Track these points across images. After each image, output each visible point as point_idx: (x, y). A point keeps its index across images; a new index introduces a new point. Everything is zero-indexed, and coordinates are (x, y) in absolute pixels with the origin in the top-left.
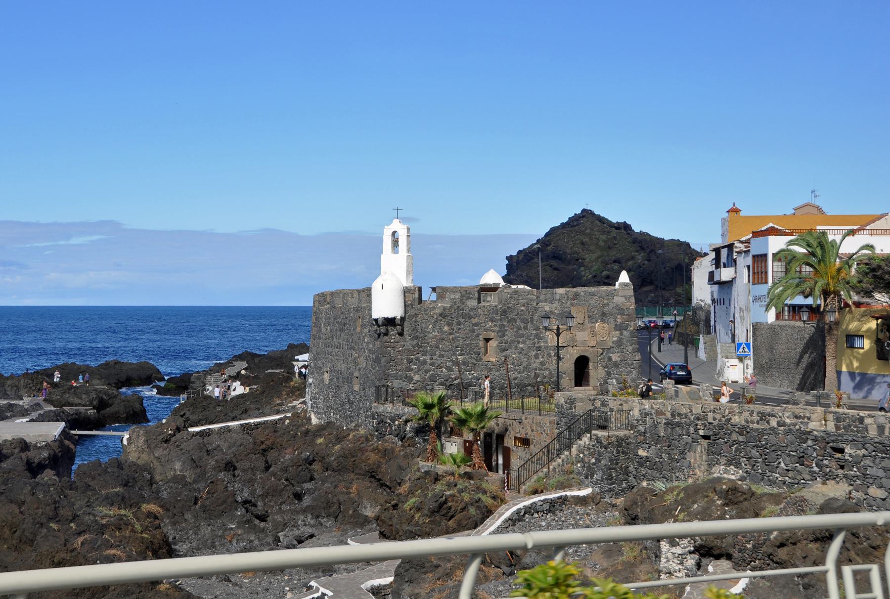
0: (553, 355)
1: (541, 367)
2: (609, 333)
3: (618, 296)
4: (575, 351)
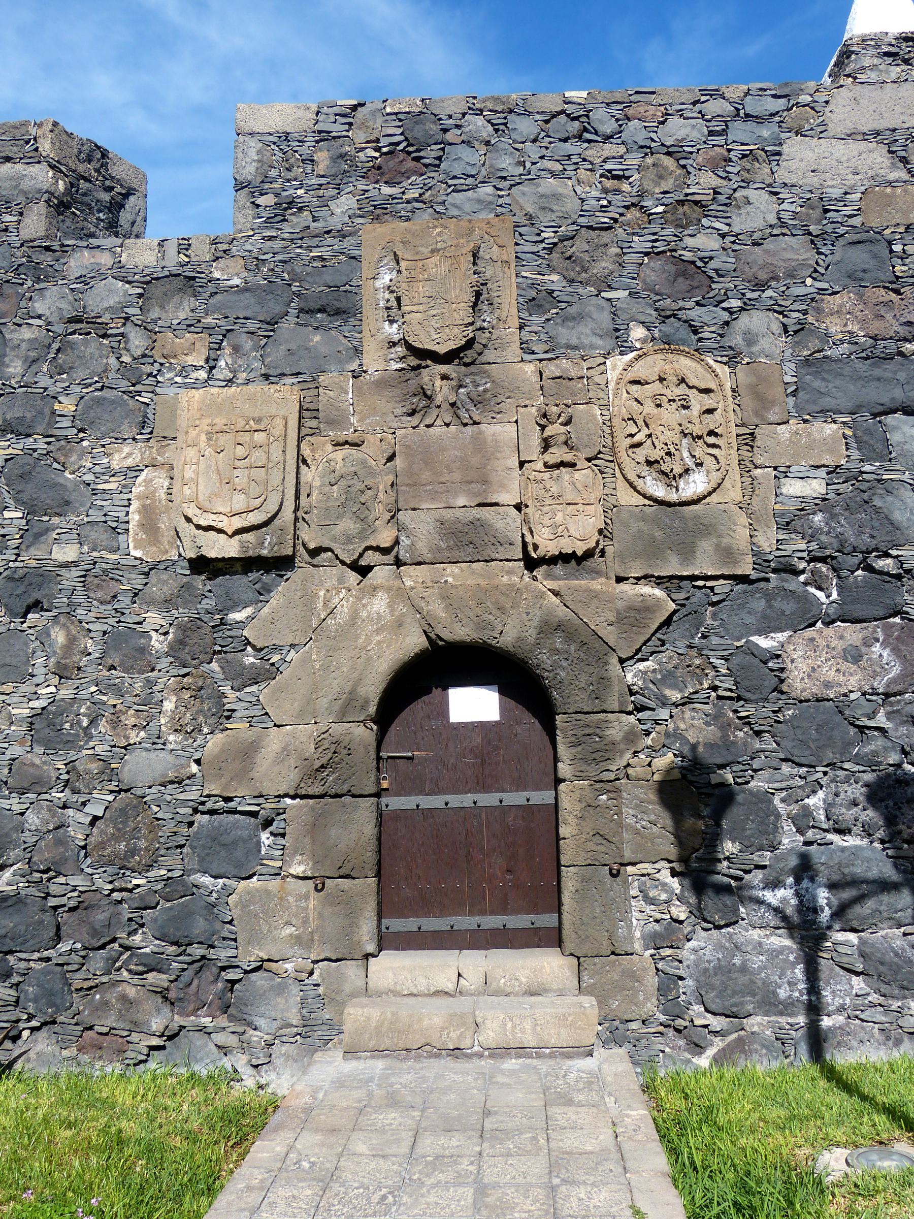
0: (157, 643)
1: (37, 756)
2: (749, 440)
3: (822, 131)
4: (379, 604)
